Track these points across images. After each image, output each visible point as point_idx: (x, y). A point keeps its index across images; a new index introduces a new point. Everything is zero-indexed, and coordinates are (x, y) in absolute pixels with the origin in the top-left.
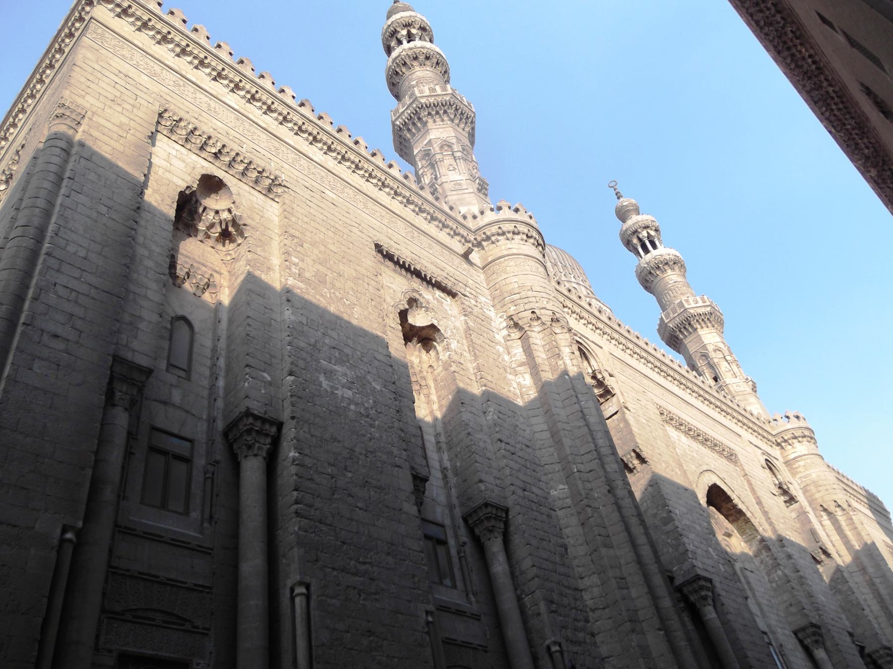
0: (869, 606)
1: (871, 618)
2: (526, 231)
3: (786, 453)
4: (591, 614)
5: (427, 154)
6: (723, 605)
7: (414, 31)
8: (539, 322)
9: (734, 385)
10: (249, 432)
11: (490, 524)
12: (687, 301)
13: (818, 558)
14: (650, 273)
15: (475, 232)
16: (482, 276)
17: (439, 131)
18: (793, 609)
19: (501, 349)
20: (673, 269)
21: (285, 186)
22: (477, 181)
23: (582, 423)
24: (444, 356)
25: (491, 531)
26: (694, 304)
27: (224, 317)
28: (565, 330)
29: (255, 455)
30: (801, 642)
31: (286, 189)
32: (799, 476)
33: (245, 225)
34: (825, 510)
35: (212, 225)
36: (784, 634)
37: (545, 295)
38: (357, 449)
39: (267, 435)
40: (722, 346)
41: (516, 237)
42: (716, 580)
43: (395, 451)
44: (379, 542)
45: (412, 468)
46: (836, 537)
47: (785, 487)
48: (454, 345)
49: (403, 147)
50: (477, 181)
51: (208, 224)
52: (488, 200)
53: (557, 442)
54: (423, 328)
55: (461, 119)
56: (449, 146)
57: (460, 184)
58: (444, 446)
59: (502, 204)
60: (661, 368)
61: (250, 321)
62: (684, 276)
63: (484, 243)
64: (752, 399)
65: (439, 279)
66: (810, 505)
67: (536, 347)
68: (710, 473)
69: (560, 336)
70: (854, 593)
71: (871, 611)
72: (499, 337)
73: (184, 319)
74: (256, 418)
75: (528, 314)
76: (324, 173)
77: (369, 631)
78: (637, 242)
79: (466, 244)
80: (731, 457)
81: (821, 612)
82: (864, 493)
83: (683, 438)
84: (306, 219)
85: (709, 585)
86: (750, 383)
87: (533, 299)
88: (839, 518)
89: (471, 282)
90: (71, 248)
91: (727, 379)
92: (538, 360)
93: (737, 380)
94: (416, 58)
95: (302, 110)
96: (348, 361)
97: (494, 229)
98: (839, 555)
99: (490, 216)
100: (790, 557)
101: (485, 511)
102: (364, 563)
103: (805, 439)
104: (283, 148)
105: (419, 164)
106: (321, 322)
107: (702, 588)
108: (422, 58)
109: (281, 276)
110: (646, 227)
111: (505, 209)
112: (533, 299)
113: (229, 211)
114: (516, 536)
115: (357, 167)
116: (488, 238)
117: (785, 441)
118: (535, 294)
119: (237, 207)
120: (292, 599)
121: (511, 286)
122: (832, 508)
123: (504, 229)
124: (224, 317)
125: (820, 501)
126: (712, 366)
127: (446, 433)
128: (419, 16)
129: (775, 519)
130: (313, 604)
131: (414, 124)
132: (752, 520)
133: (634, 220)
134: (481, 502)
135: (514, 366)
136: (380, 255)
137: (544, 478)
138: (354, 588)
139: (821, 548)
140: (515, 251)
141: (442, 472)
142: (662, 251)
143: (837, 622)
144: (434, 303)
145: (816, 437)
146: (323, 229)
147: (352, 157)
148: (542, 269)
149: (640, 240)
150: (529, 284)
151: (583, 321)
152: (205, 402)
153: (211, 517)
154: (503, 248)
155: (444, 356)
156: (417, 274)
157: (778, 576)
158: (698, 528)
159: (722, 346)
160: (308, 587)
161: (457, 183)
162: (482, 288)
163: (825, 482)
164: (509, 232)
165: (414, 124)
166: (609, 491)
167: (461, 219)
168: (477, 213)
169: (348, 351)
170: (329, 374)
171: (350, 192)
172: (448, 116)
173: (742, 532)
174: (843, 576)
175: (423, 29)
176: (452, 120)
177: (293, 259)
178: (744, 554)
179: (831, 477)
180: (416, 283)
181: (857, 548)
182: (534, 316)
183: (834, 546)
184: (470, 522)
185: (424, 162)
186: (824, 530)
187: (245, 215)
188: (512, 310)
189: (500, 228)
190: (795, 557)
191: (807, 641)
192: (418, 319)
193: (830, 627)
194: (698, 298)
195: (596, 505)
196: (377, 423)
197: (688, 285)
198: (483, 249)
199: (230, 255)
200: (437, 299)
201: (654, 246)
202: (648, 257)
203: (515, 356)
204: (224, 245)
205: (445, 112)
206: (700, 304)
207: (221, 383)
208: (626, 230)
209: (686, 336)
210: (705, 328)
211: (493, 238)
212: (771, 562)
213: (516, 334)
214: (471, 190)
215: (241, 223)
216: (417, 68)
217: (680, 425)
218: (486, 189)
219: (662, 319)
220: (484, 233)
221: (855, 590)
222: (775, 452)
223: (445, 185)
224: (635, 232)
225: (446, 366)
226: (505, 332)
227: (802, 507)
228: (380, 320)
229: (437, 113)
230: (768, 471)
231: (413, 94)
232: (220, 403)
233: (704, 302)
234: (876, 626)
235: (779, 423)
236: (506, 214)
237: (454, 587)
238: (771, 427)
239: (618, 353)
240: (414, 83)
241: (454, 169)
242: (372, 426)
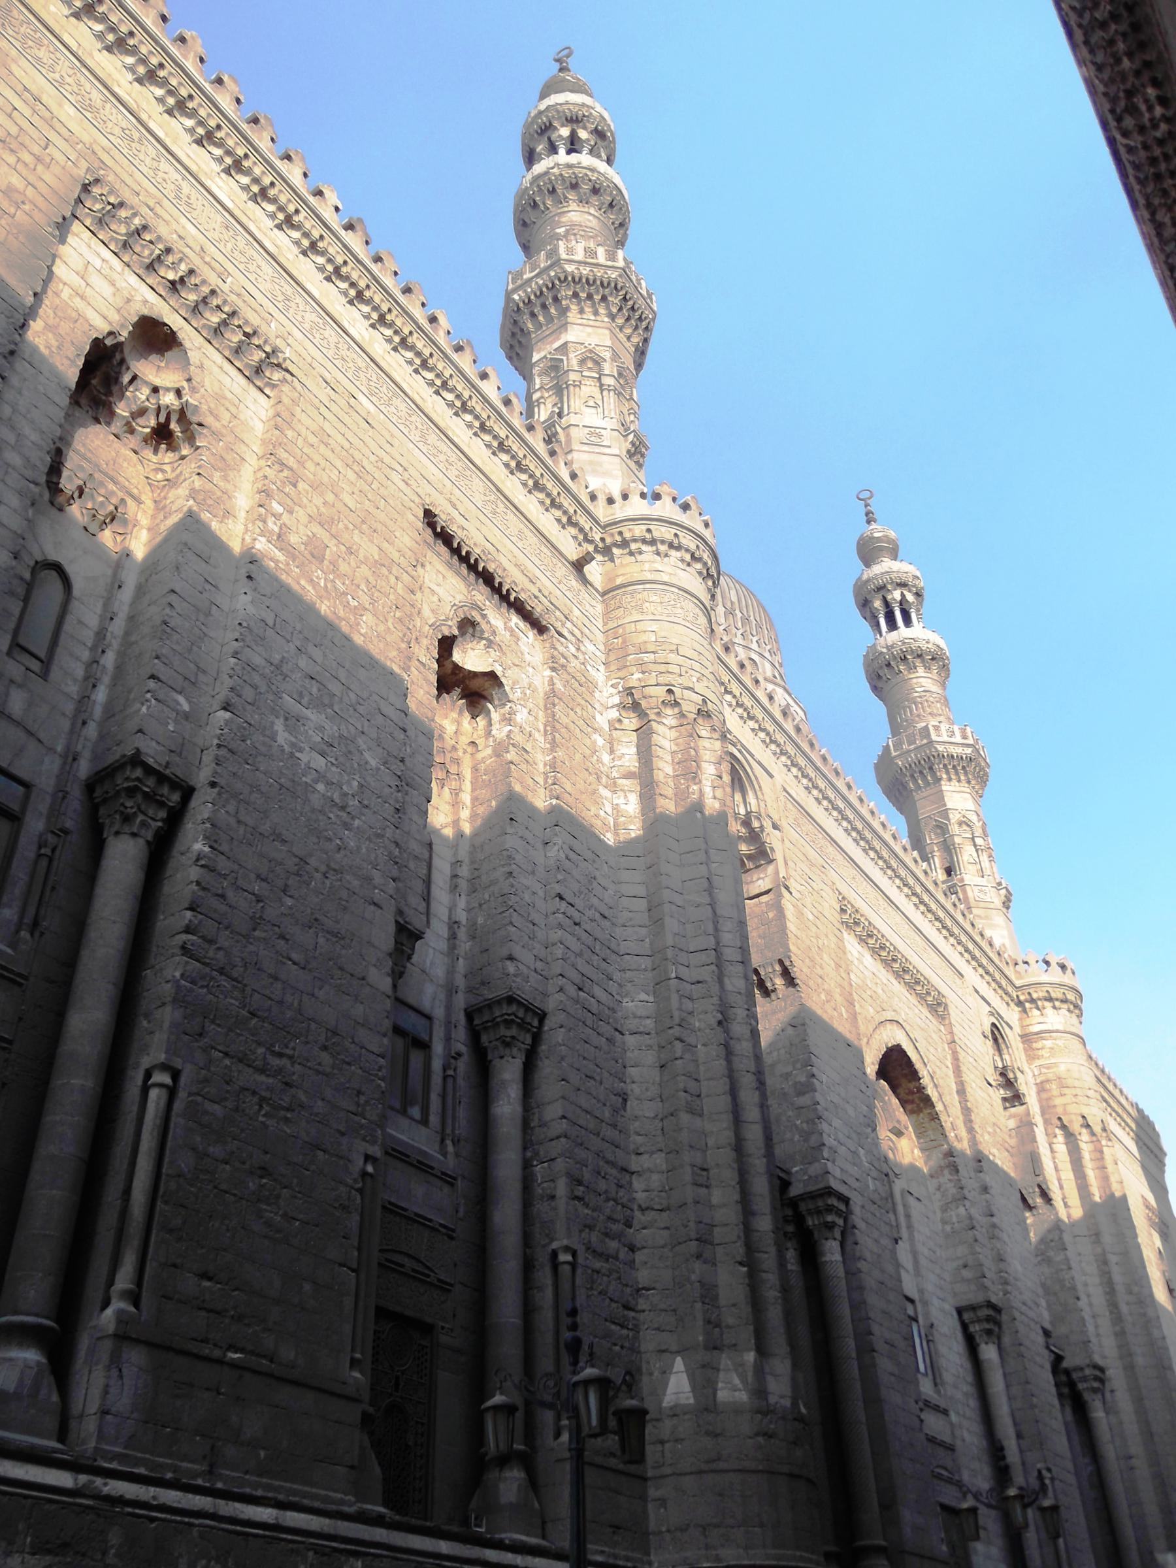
0: (1089, 1296)
1: (1087, 1314)
2: (693, 547)
3: (1028, 1022)
4: (637, 1214)
5: (554, 367)
6: (856, 1244)
7: (583, 134)
8: (676, 710)
10: (131, 792)
11: (509, 1033)
12: (937, 728)
13: (1030, 1201)
14: (888, 665)
15: (604, 527)
16: (599, 608)
17: (587, 331)
18: (967, 1274)
19: (600, 741)
20: (928, 669)
21: (287, 371)
22: (631, 437)
23: (706, 899)
24: (500, 731)
25: (507, 1045)
26: (947, 736)
27: (130, 581)
28: (716, 736)
29: (134, 835)
30: (965, 1326)
31: (288, 376)
32: (1038, 1062)
33: (200, 425)
34: (1064, 1127)
35: (142, 412)
36: (943, 1310)
37: (697, 666)
38: (313, 862)
39: (162, 804)
40: (974, 818)
41: (673, 553)
42: (856, 1200)
43: (378, 878)
44: (313, 1026)
45: (400, 912)
46: (1068, 1175)
47: (1011, 1076)
48: (521, 716)
49: (516, 345)
50: (631, 437)
51: (134, 408)
52: (641, 475)
53: (656, 919)
54: (475, 675)
55: (628, 319)
56: (597, 363)
57: (600, 436)
58: (463, 885)
59: (664, 490)
60: (864, 834)
61: (173, 598)
62: (943, 685)
63: (615, 551)
64: (999, 919)
65: (522, 596)
66: (1043, 1113)
67: (660, 752)
68: (895, 1026)
69: (706, 743)
70: (1070, 1268)
71: (1091, 1305)
72: (602, 721)
73: (58, 568)
74: (149, 770)
75: (661, 692)
76: (362, 362)
77: (263, 1168)
78: (881, 605)
79: (585, 545)
80: (938, 1007)
81: (1009, 1288)
82: (1134, 1113)
83: (868, 959)
84: (312, 439)
85: (842, 1207)
86: (1004, 892)
87: (676, 669)
88: (1083, 1145)
89: (576, 612)
91: (968, 875)
92: (659, 776)
93: (983, 881)
94: (574, 186)
95: (348, 237)
96: (331, 706)
97: (639, 530)
98: (1066, 1204)
99: (638, 507)
100: (985, 1189)
101: (505, 1009)
102: (280, 1055)
103: (1065, 1006)
104: (299, 300)
105: (538, 381)
106: (299, 627)
107: (830, 1209)
108: (586, 187)
109: (247, 530)
110: (903, 585)
111: (666, 500)
112: (676, 669)
113: (178, 393)
114: (546, 1062)
115: (424, 364)
116: (625, 544)
117: (1033, 1001)
118: (681, 660)
119: (194, 390)
120: (145, 1090)
121: (643, 638)
122: (1076, 1126)
123: (656, 534)
124: (130, 581)
125: (1060, 1110)
126: (949, 848)
127: (472, 862)
128: (599, 108)
129: (981, 1124)
130: (178, 1106)
131: (544, 306)
132: (943, 1118)
133: (885, 566)
134: (502, 992)
135: (615, 774)
136: (429, 531)
137: (617, 976)
138: (254, 1093)
139: (1039, 1186)
140: (666, 578)
141: (450, 928)
142: (918, 633)
143: (1029, 1307)
144: (503, 636)
145: (1083, 1006)
146: (339, 464)
147: (420, 345)
148: (703, 620)
149: (887, 604)
150: (675, 641)
151: (751, 724)
152: (66, 725)
153: (35, 924)
154: (647, 567)
155: (500, 731)
156: (487, 578)
157: (958, 1215)
158: (851, 1112)
159: (974, 818)
160: (176, 1075)
161: (594, 431)
162: (593, 628)
163: (1076, 1083)
164: (663, 542)
165: (544, 306)
166: (720, 1023)
167: (585, 499)
168: (617, 496)
169: (334, 687)
170: (293, 721)
171: (402, 406)
172: (608, 308)
173: (920, 1133)
174: (1061, 1238)
175: (600, 134)
176: (613, 317)
177: (275, 505)
178: (913, 1167)
179: (1087, 1078)
180: (481, 595)
181: (1097, 1199)
182: (670, 698)
183: (1061, 1187)
184: (476, 1022)
185: (546, 379)
186: (1054, 1158)
187: (204, 407)
188: (636, 678)
189: (649, 531)
190: (992, 1191)
191: (975, 1328)
192: (470, 658)
193: (1017, 1314)
194: (956, 729)
195: (691, 1040)
196: (357, 822)
197: (946, 702)
198: (612, 560)
199: (163, 471)
200: (512, 631)
201: (908, 621)
202: (892, 637)
203: (620, 758)
204: (156, 451)
205: (604, 299)
206: (958, 738)
207: (101, 695)
208: (869, 580)
209: (919, 788)
210: (954, 783)
211: (633, 546)
212: (954, 1191)
213: (631, 722)
214: (616, 452)
215: (194, 419)
216: (573, 206)
218: (643, 455)
219: (887, 748)
220: (620, 533)
221: (1073, 1265)
222: (1011, 1015)
223: (573, 430)
224: (881, 588)
225: (500, 749)
226: (614, 714)
227: (1028, 1114)
228: (404, 646)
229: (590, 297)
230: (990, 1043)
231: (554, 252)
232: (91, 731)
233: (965, 737)
234: (1091, 1328)
235: (1030, 970)
236: (666, 508)
237: (425, 1122)
238: (1016, 972)
239: (798, 792)
240: (561, 230)
241: (596, 406)
242: (346, 826)
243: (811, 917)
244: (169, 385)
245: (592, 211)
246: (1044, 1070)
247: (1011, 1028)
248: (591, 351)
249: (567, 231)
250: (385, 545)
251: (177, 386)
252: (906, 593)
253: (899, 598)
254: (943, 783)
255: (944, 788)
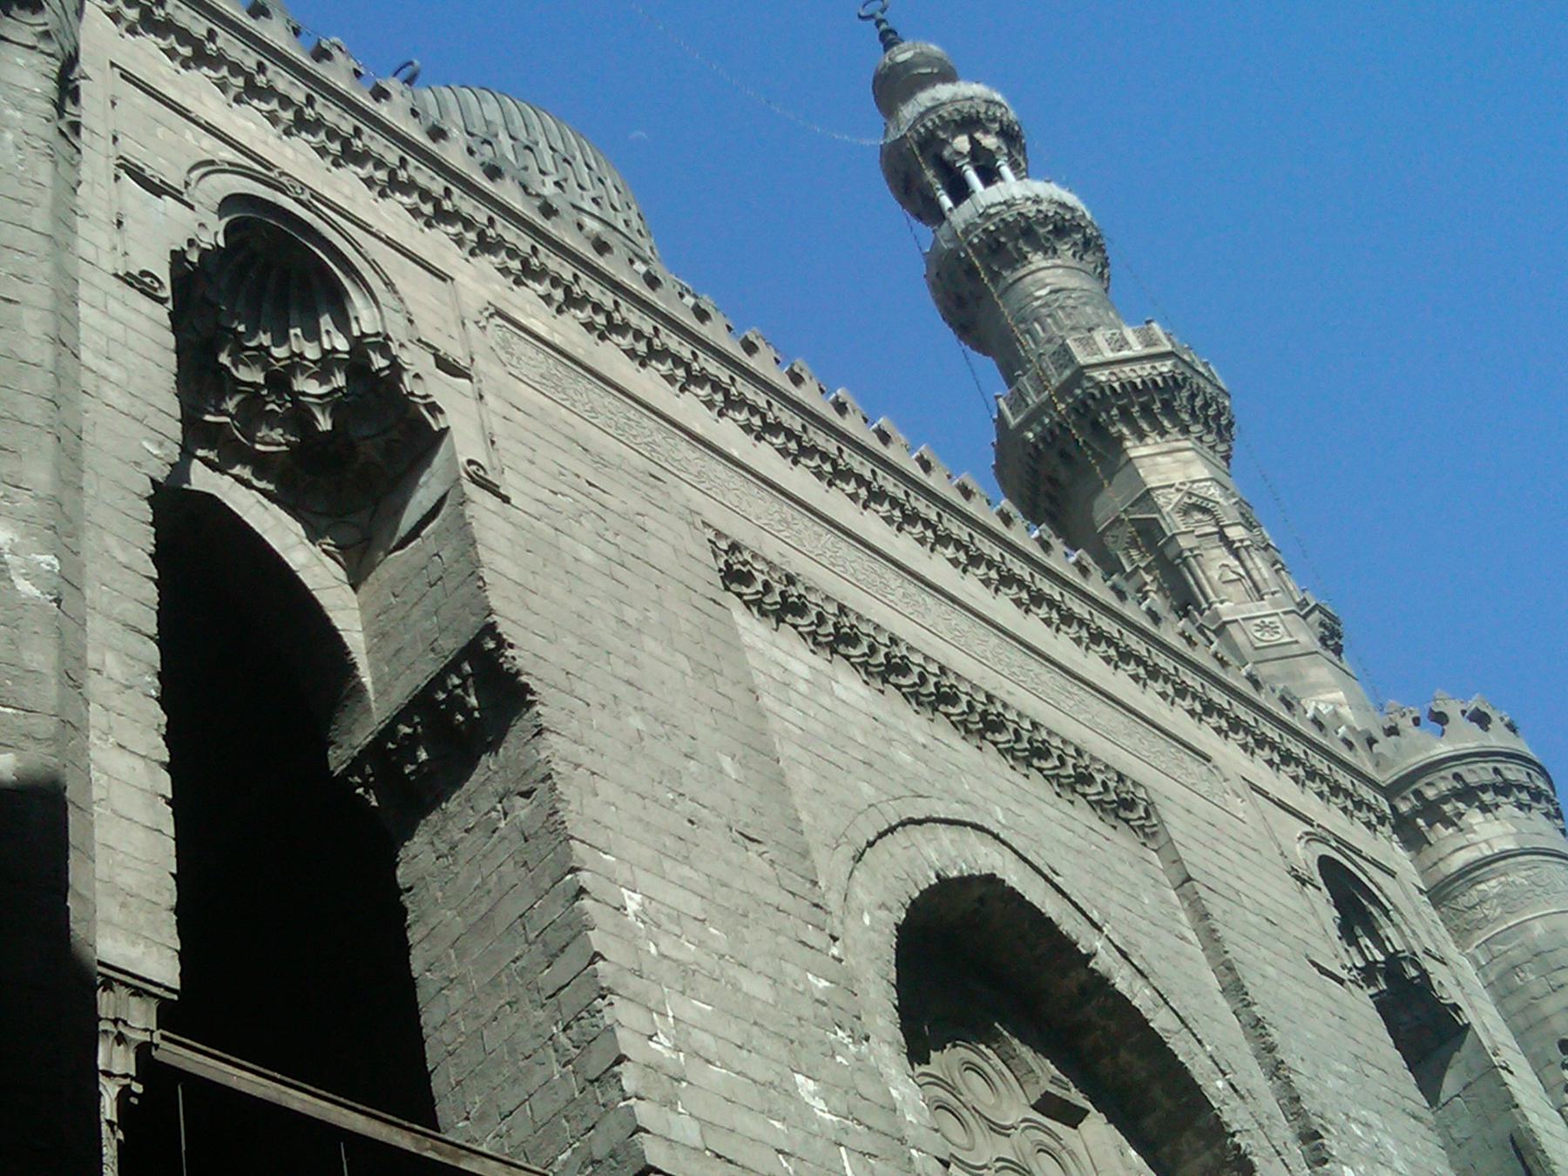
9: (1251, 626)
40: (1214, 492)
64: (1320, 671)
93: (1265, 607)
159: (1214, 492)
217: (839, 638)
219: (1001, 421)
233: (1149, 341)
243: (588, 555)
246: (1496, 948)
247: (1392, 874)
252: (978, 135)
254: (1128, 444)
255: (1133, 453)
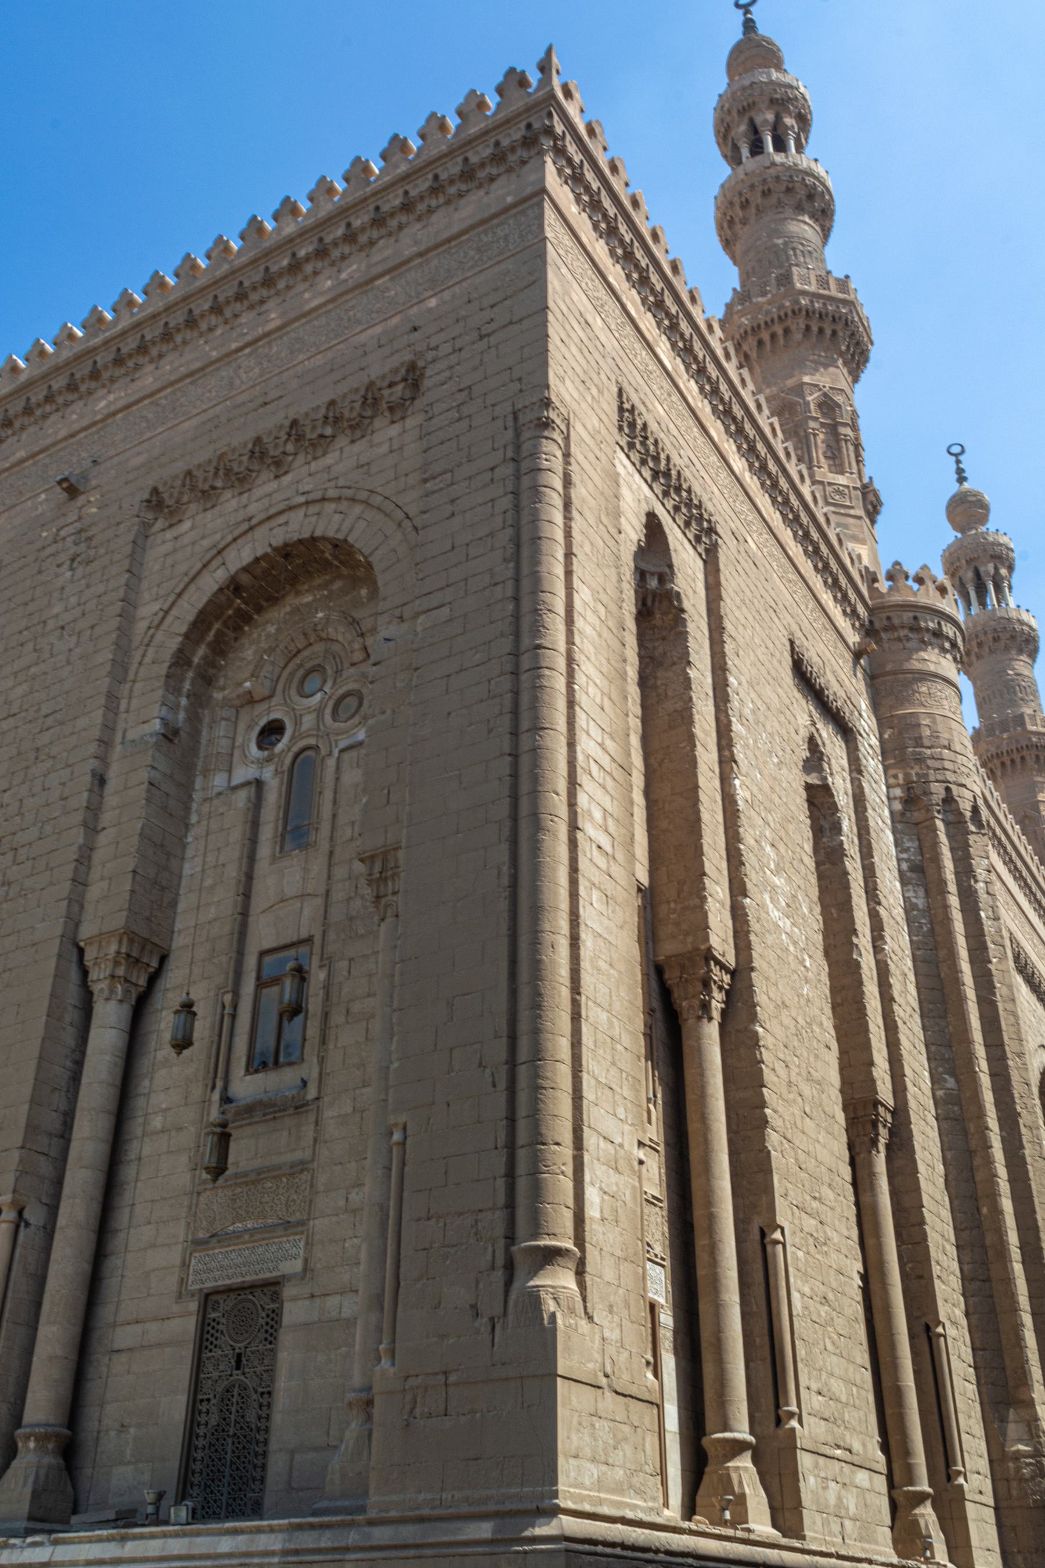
2: (951, 634)
7: (789, 121)
12: (1033, 717)
63: (883, 635)
90: (592, 690)
108: (802, 193)
112: (947, 765)
149: (978, 574)
168: (882, 576)
189: (915, 618)
205: (834, 333)
211: (902, 633)
220: (889, 618)
244: (653, 569)
245: (807, 220)
248: (825, 395)
249: (785, 244)
250: (780, 691)
251: (659, 570)
253: (992, 571)
